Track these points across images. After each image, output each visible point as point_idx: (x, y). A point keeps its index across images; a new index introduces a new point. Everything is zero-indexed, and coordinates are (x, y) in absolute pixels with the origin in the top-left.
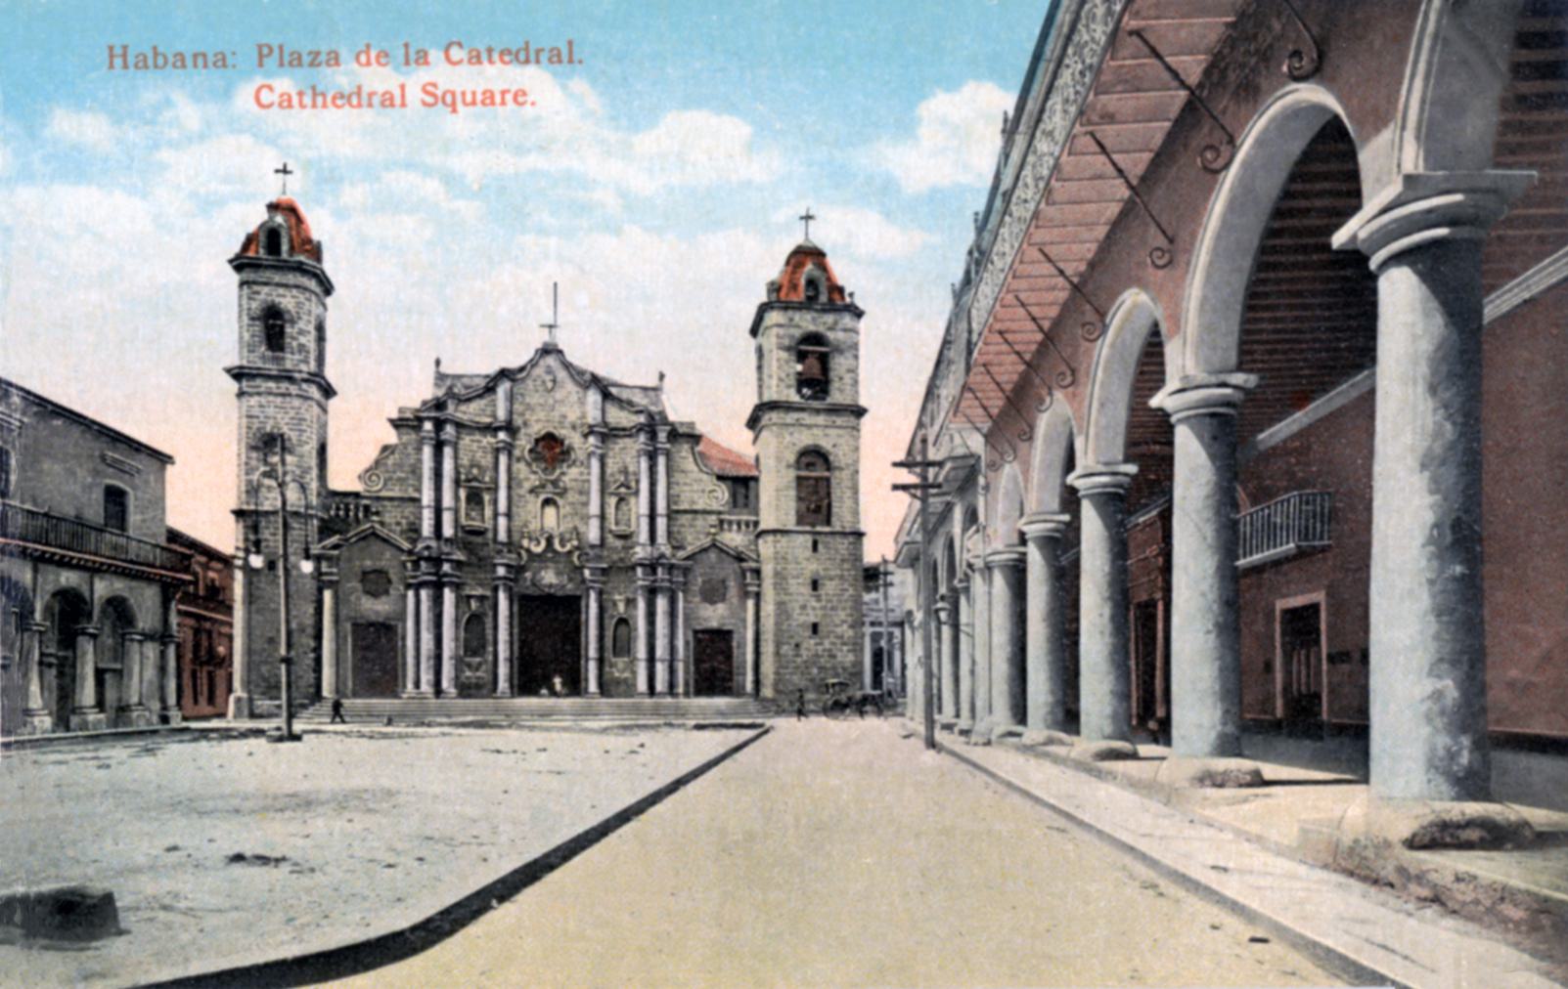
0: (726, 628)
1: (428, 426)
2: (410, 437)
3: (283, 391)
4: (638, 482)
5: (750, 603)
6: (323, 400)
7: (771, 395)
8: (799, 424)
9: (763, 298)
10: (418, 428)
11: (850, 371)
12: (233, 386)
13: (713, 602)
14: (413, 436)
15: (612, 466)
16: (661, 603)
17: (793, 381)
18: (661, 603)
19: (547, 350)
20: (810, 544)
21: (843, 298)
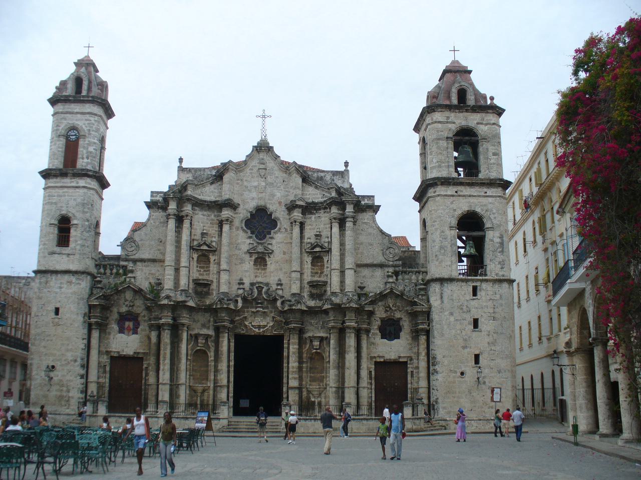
0: (401, 360)
1: (173, 206)
2: (160, 214)
3: (74, 184)
4: (330, 243)
5: (423, 339)
6: (99, 190)
7: (432, 174)
8: (457, 195)
9: (424, 104)
10: (164, 208)
11: (494, 154)
12: (42, 181)
13: (391, 339)
14: (165, 214)
15: (309, 233)
16: (351, 341)
17: (452, 163)
18: (351, 341)
19: (263, 148)
20: (471, 289)
21: (486, 101)
